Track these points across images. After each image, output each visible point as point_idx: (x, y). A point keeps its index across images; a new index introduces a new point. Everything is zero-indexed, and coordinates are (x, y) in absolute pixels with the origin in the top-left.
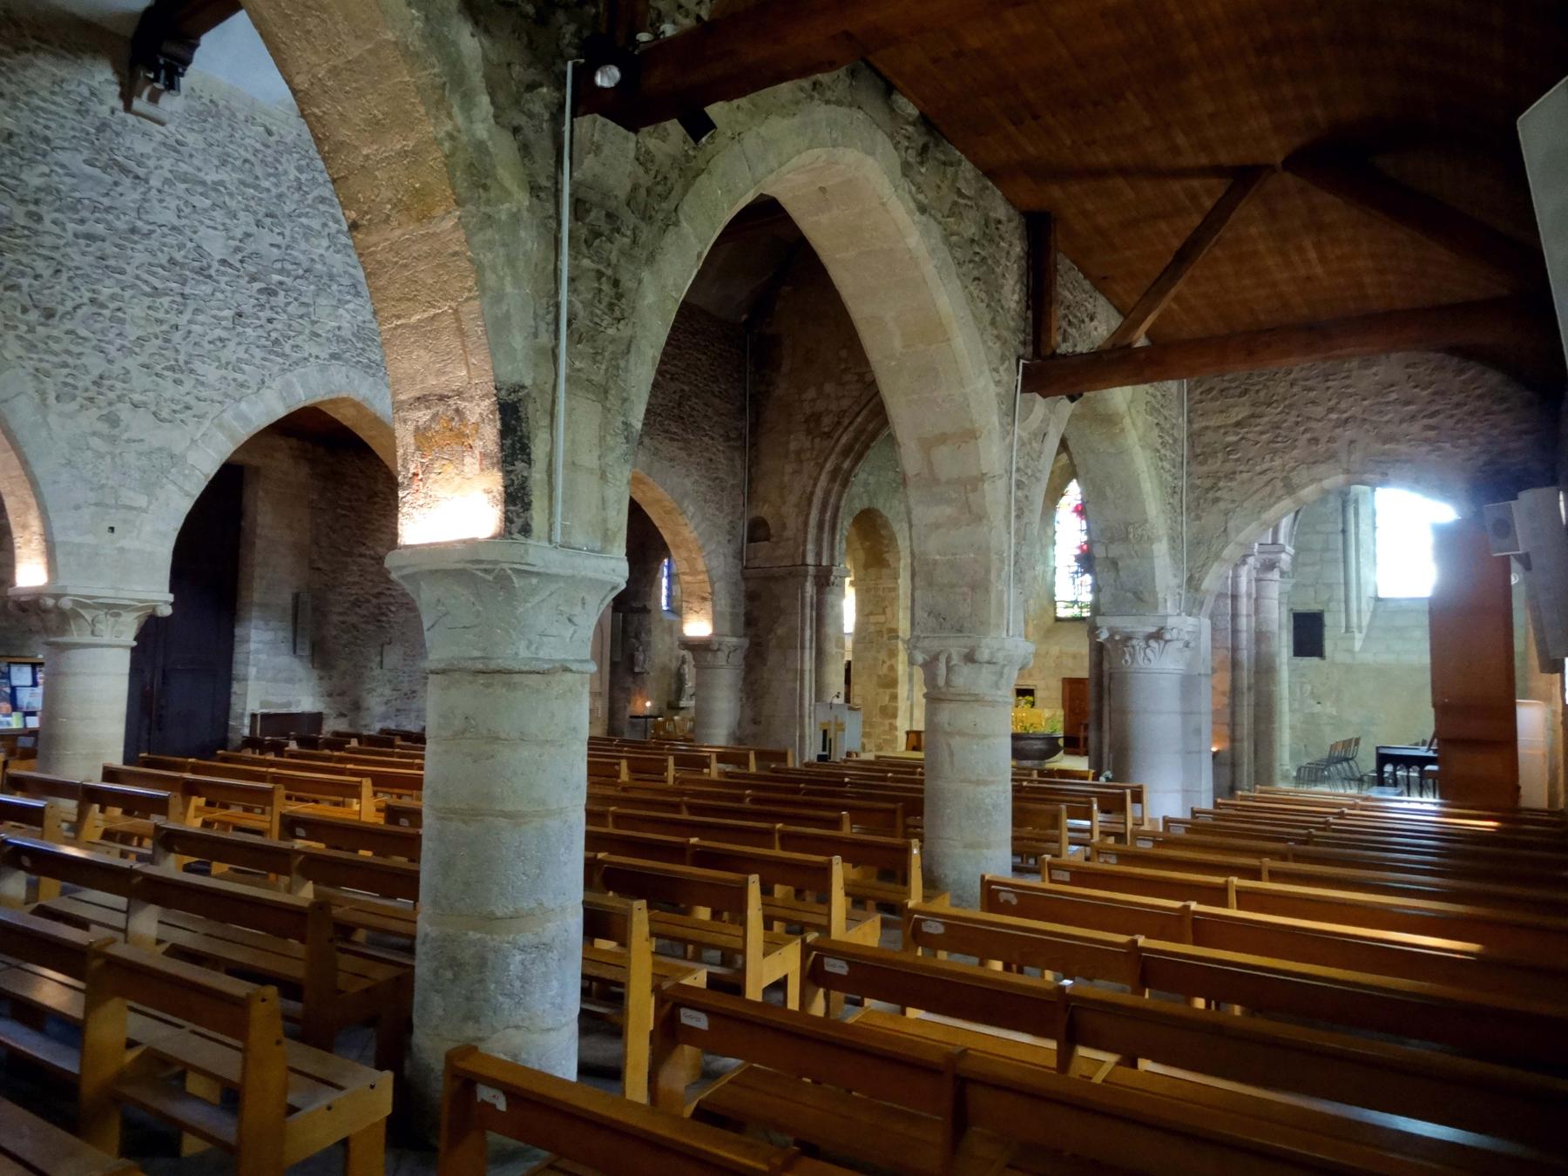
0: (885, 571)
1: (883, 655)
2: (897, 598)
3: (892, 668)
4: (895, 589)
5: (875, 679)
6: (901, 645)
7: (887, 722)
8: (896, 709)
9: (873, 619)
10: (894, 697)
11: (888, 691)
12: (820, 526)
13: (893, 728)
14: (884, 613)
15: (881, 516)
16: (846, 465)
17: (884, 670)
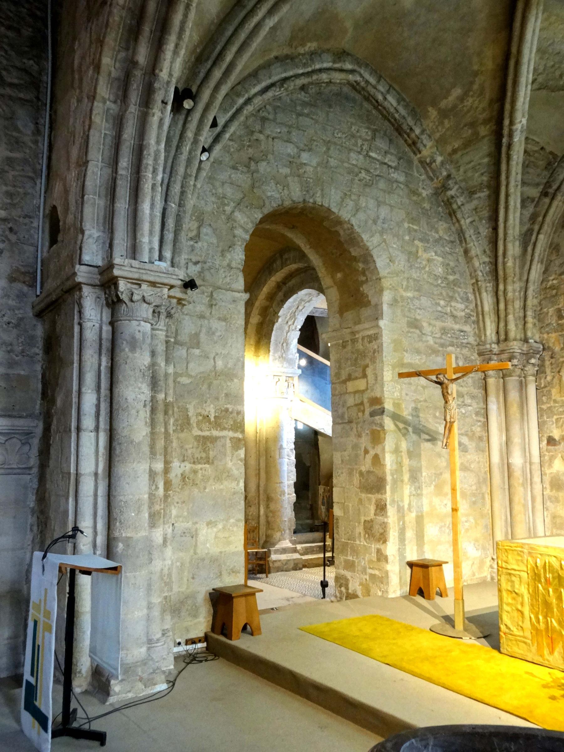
0: (366, 312)
1: (365, 441)
2: (379, 350)
3: (377, 460)
4: (376, 337)
5: (356, 479)
6: (388, 423)
7: (374, 546)
8: (384, 526)
9: (351, 386)
10: (381, 508)
11: (374, 497)
12: (112, 193)
13: (382, 557)
14: (365, 376)
15: (339, 222)
16: (142, 55)
17: (366, 465)
